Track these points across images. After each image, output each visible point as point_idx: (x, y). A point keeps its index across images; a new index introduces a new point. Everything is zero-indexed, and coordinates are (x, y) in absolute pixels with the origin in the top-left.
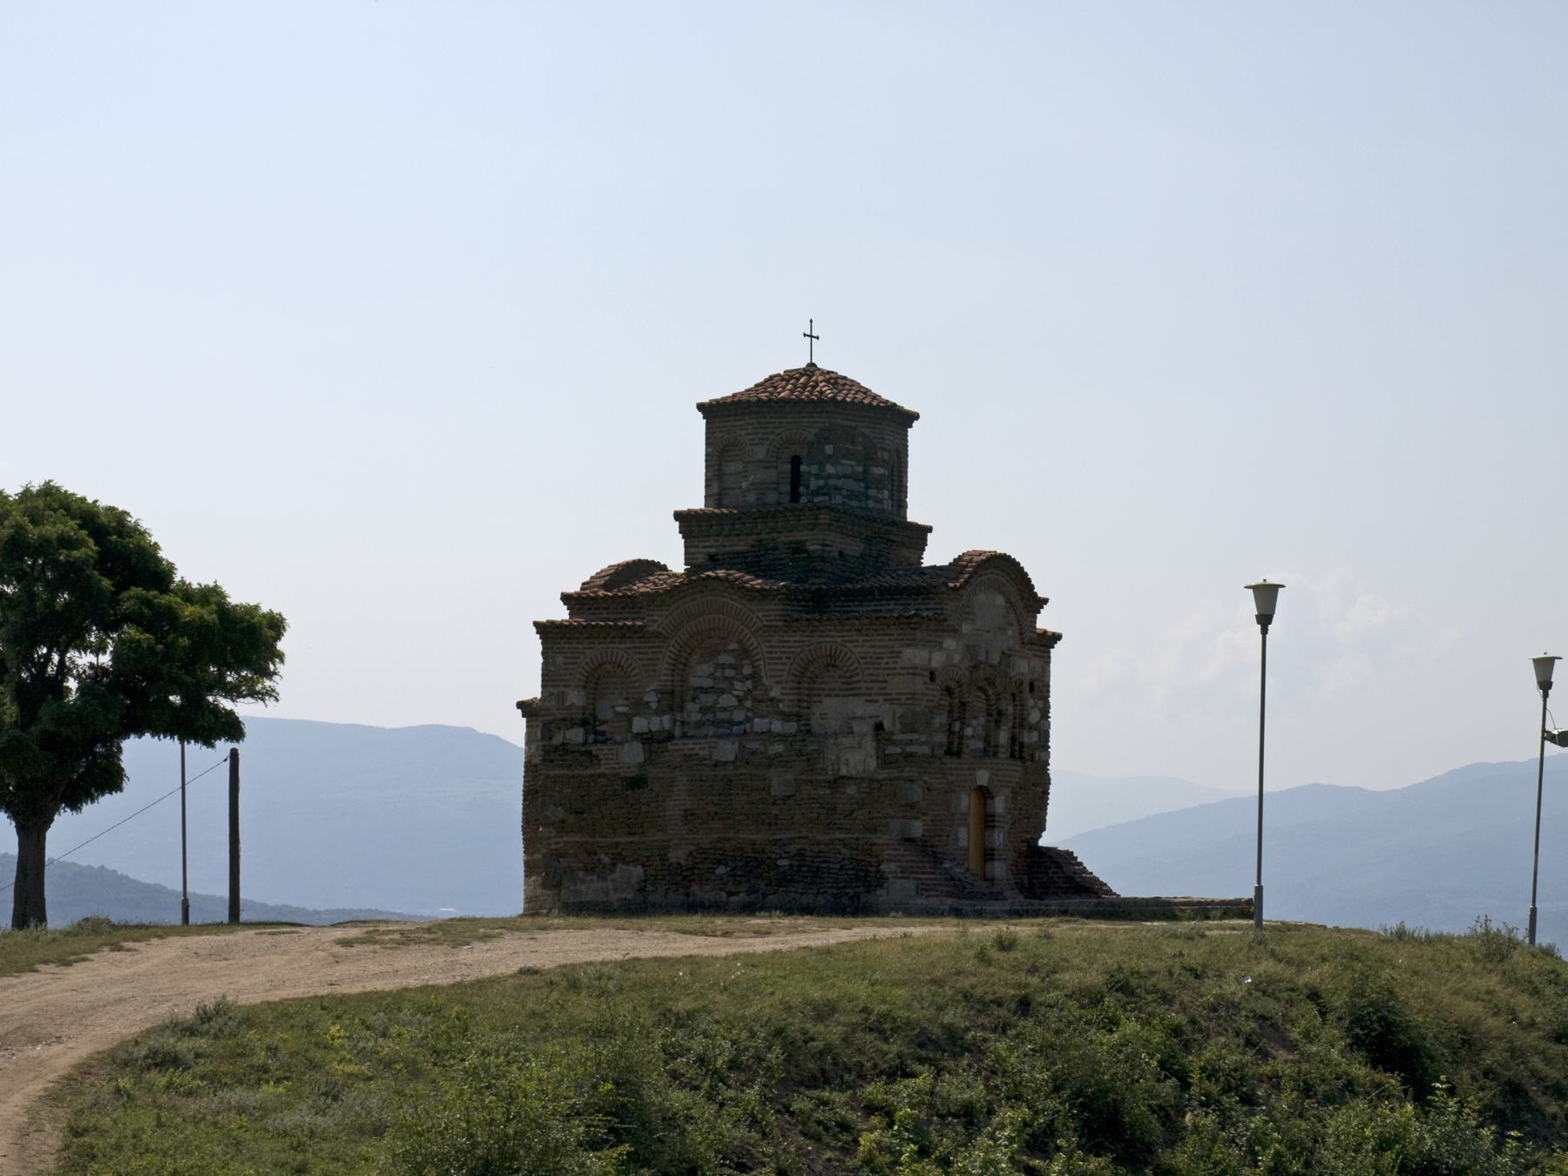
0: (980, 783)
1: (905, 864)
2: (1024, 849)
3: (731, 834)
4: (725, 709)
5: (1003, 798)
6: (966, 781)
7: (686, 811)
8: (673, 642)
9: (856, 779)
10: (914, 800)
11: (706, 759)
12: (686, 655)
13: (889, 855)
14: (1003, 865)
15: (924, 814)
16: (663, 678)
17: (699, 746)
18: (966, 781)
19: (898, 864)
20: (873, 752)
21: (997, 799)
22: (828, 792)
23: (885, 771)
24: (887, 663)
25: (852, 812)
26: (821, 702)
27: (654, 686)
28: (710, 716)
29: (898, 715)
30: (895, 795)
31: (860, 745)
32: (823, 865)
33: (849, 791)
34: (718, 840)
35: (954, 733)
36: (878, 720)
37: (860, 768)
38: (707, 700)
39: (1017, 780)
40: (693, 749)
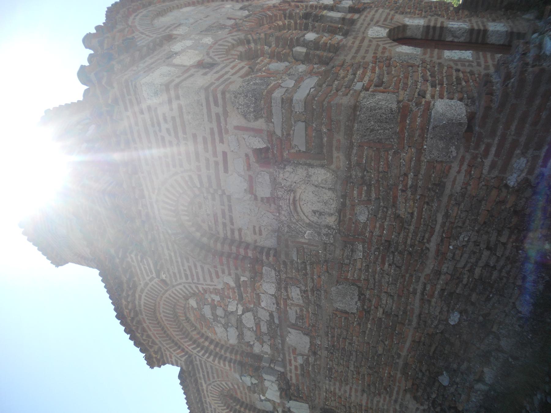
1: (523, 139)
2: (466, 12)
3: (401, 362)
4: (258, 325)
6: (378, 46)
7: (363, 391)
8: (195, 351)
9: (344, 204)
10: (394, 106)
11: (307, 359)
12: (207, 344)
13: (493, 166)
14: (490, 24)
15: (422, 95)
16: (227, 367)
17: (293, 362)
19: (518, 151)
20: (301, 172)
21: (408, 23)
22: (360, 247)
23: (335, 154)
24: (168, 130)
25: (397, 217)
26: (240, 230)
27: (237, 376)
28: (266, 338)
29: (243, 122)
30: (380, 141)
31: (291, 190)
32: (478, 271)
33: (363, 218)
34: (404, 373)
35: (307, 54)
36: (252, 159)
37: (328, 195)
38: (249, 336)
40: (296, 367)
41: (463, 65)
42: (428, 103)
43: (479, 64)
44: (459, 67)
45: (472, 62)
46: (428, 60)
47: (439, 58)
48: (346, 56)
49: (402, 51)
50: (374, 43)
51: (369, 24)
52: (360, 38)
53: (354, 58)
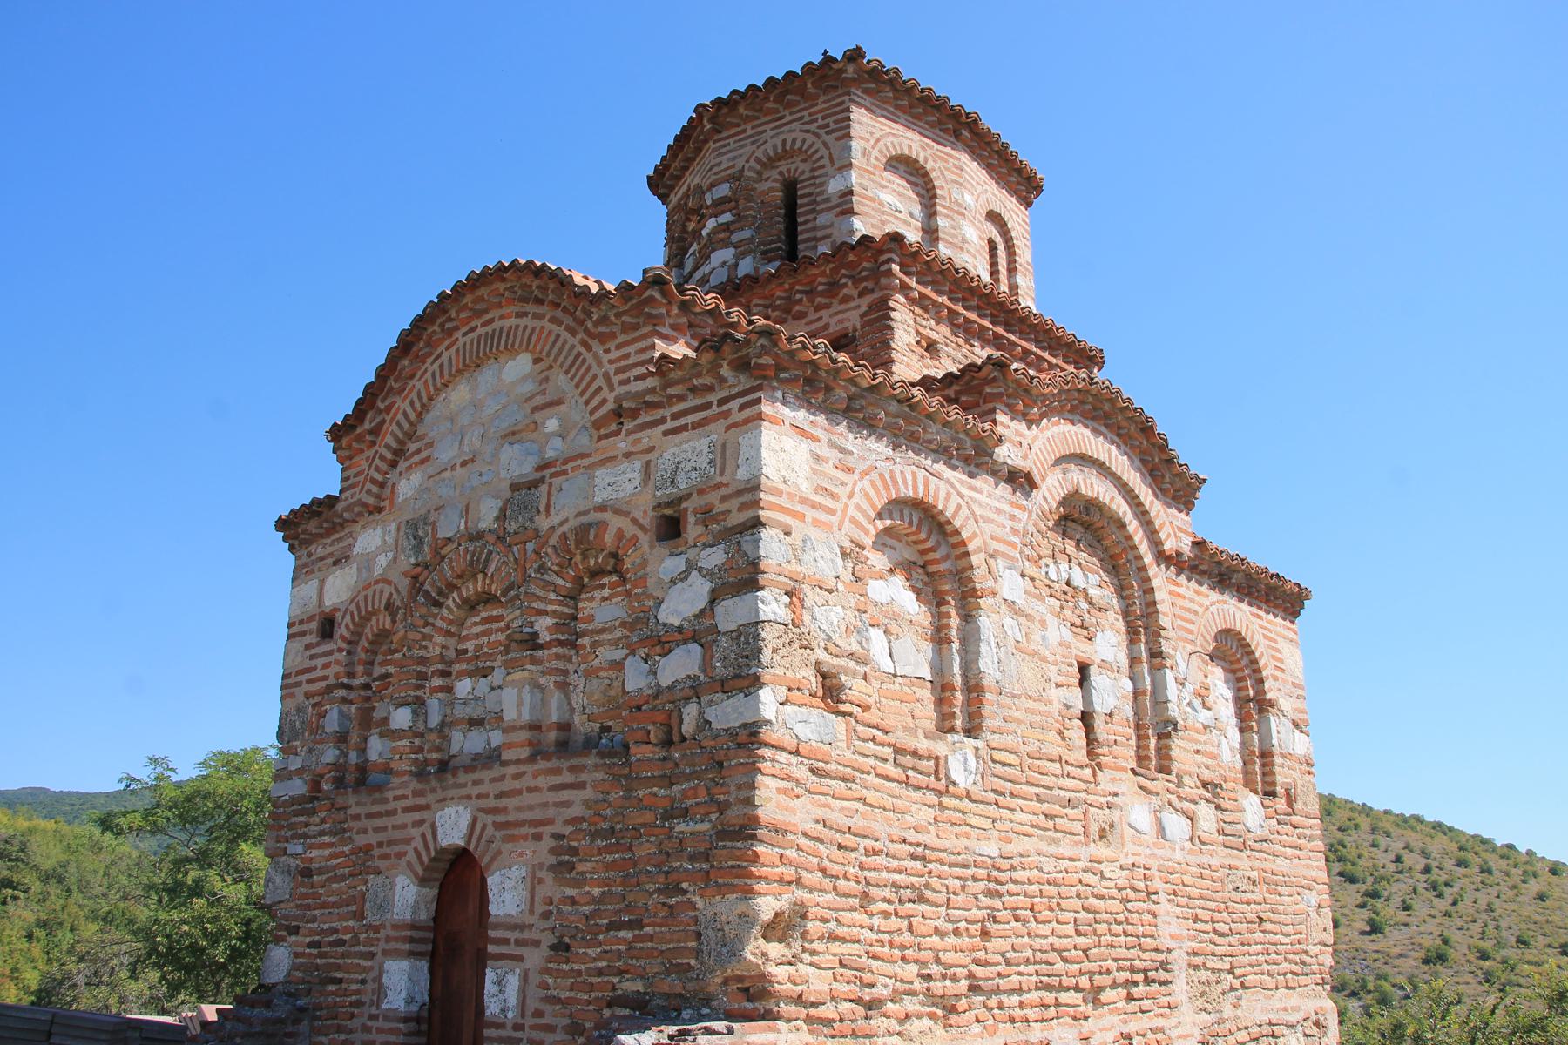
0: (445, 841)
5: (518, 872)
6: (408, 841)
18: (408, 841)
39: (577, 811)
41: (373, 990)
42: (283, 939)
43: (373, 1017)
44: (370, 986)
45: (378, 1007)
46: (382, 934)
47: (385, 953)
48: (357, 804)
49: (399, 888)
50: (415, 832)
51: (469, 797)
52: (421, 801)
53: (357, 817)
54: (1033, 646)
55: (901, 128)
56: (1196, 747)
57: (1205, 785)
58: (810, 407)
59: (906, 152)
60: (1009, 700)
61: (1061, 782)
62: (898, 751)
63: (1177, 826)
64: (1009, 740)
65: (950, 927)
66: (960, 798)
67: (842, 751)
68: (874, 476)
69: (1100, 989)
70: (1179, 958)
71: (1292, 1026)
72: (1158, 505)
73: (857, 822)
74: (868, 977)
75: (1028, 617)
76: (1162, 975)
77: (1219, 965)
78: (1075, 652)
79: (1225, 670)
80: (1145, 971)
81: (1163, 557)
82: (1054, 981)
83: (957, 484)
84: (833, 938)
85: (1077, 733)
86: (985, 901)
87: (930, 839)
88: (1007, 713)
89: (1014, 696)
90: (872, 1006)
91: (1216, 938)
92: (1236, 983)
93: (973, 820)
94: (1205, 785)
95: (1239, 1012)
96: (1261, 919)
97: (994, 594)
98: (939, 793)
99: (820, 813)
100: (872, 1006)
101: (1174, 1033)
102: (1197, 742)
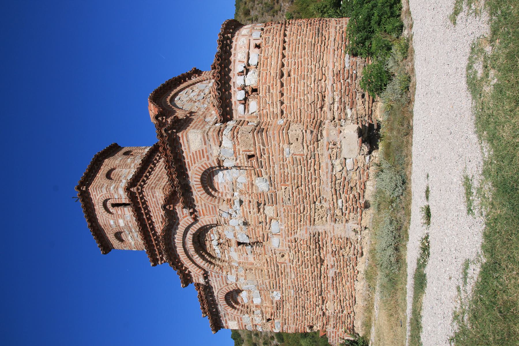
54: (244, 275)
55: (109, 239)
56: (249, 213)
57: (259, 211)
58: (221, 321)
59: (115, 238)
60: (259, 283)
61: (273, 269)
62: (277, 309)
63: (275, 227)
64: (267, 284)
65: (309, 300)
66: (283, 296)
67: (280, 320)
68: (226, 308)
69: (321, 258)
70: (312, 229)
71: (333, 167)
72: (181, 223)
73: (292, 318)
74: (319, 316)
75: (237, 275)
76: (317, 236)
77: (313, 210)
78: (236, 247)
79: (214, 176)
80: (316, 243)
81: (196, 220)
82: (319, 275)
83: (217, 292)
84: (313, 321)
85: (258, 249)
86: (303, 292)
87: (292, 304)
88: (262, 284)
89: (257, 282)
90: (324, 314)
91: (306, 211)
92: (319, 199)
93: (287, 295)
94: (259, 211)
95: (328, 199)
96: (298, 187)
97: (236, 284)
98: (283, 301)
99: (292, 324)
100: (324, 314)
101: (332, 234)
102: (247, 213)
